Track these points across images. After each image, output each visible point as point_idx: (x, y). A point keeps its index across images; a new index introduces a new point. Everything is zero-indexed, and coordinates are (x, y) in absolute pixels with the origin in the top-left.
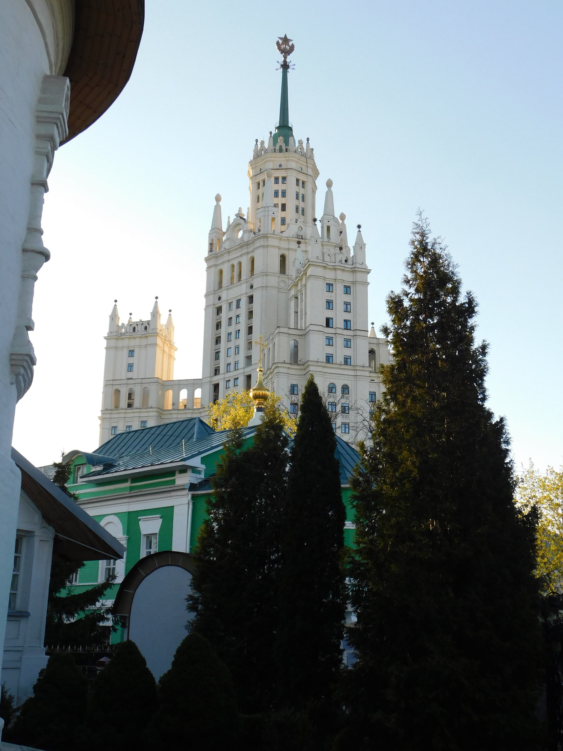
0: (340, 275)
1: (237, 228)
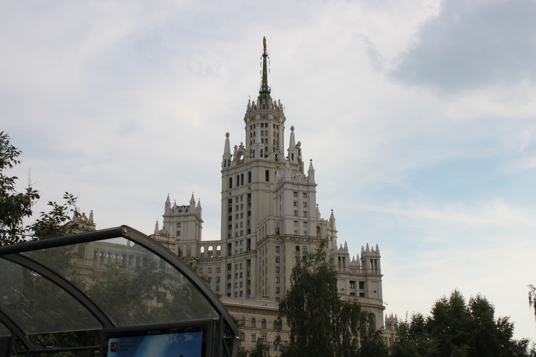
0: (301, 188)
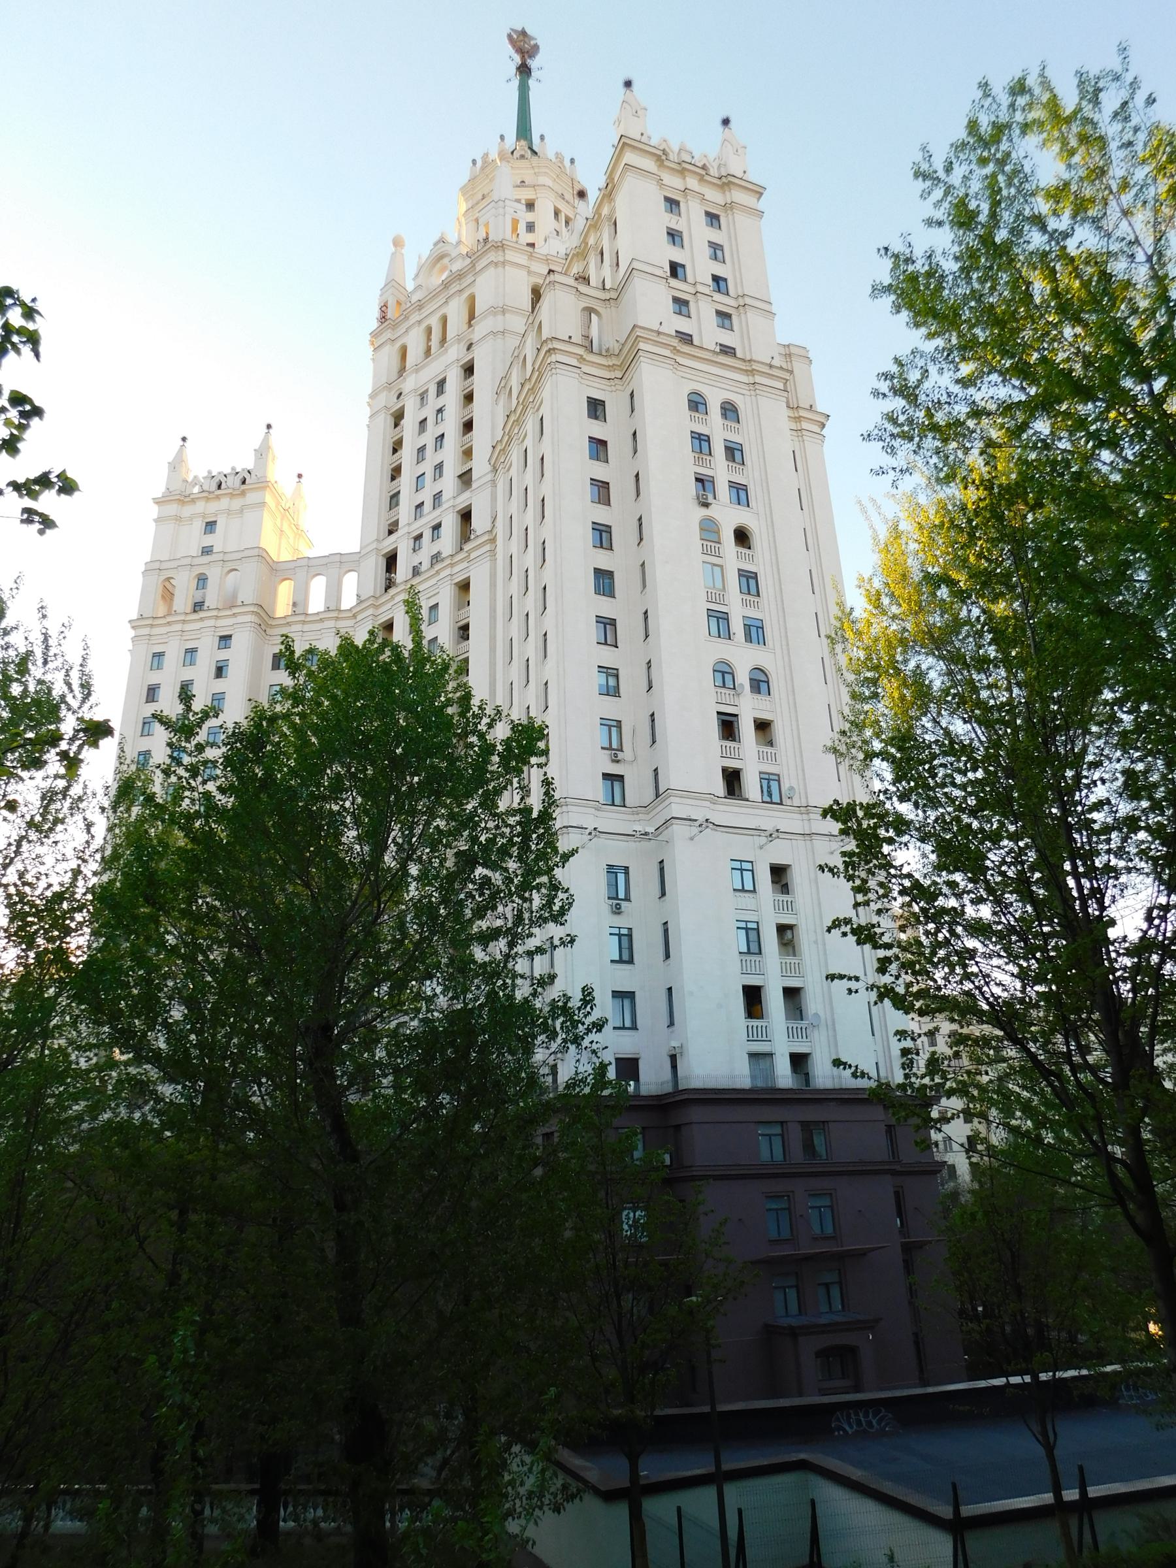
1: (438, 265)
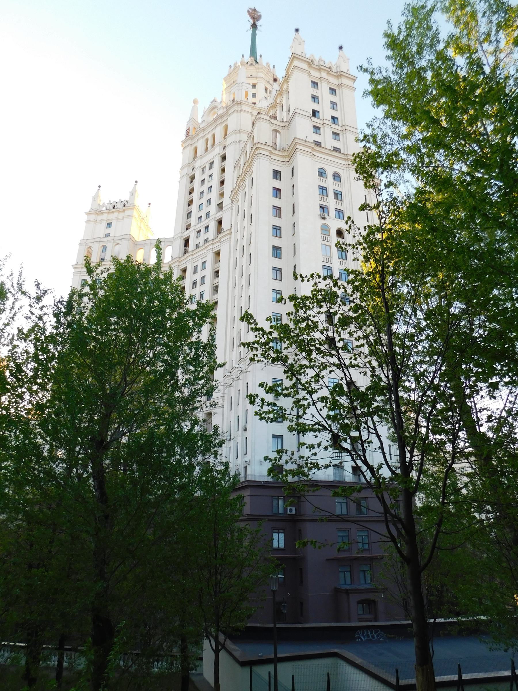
1: (213, 112)
